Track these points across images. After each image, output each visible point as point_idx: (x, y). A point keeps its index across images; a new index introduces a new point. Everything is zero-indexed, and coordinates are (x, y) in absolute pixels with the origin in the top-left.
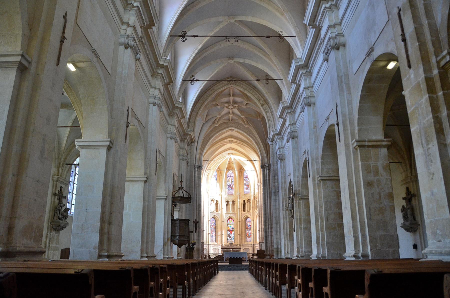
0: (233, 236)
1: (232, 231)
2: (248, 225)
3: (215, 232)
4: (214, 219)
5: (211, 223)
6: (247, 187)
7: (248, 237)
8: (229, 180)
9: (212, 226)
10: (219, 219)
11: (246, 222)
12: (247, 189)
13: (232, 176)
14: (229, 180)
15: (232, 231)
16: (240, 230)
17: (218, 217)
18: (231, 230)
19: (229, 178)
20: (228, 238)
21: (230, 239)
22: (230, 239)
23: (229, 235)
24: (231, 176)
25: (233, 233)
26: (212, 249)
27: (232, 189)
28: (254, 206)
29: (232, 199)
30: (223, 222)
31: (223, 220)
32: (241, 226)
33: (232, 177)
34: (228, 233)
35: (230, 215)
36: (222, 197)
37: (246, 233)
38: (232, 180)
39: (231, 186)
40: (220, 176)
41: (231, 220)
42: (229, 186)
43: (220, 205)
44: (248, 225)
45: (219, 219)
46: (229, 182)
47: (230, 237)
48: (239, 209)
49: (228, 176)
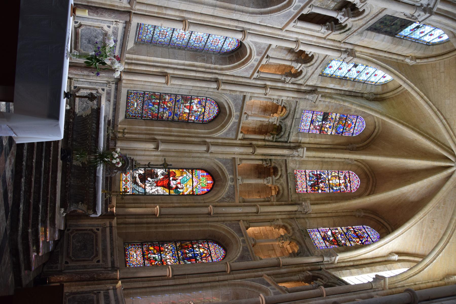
0: (148, 190)
1: (168, 187)
2: (197, 251)
3: (167, 120)
4: (215, 118)
5: (200, 103)
6: (331, 239)
7: (148, 250)
8: (335, 176)
9: (190, 109)
10: (216, 135)
11: (207, 240)
12: (324, 238)
13: (349, 189)
14: (335, 176)
15: (168, 187)
16: (175, 215)
17: (225, 130)
18: (173, 183)
19: (342, 177)
20: (142, 172)
21: (138, 180)
22: (138, 180)
23: (154, 175)
24: (349, 185)
25: (161, 190)
26: (100, 91)
27: (312, 186)
28: (283, 271)
29: (285, 185)
30: (204, 148)
31: (212, 149)
32: (194, 219)
33: (346, 186)
34: (160, 172)
35: (229, 177)
36: (289, 148)
37: (163, 242)
38: (336, 186)
39: (321, 185)
40: (350, 147)
41: (210, 182)
42: (318, 177)
43: (264, 140)
44: (197, 251)
45: (216, 135)
46: (329, 177)
47: (143, 178)
48: (254, 210)
49: (347, 175)
